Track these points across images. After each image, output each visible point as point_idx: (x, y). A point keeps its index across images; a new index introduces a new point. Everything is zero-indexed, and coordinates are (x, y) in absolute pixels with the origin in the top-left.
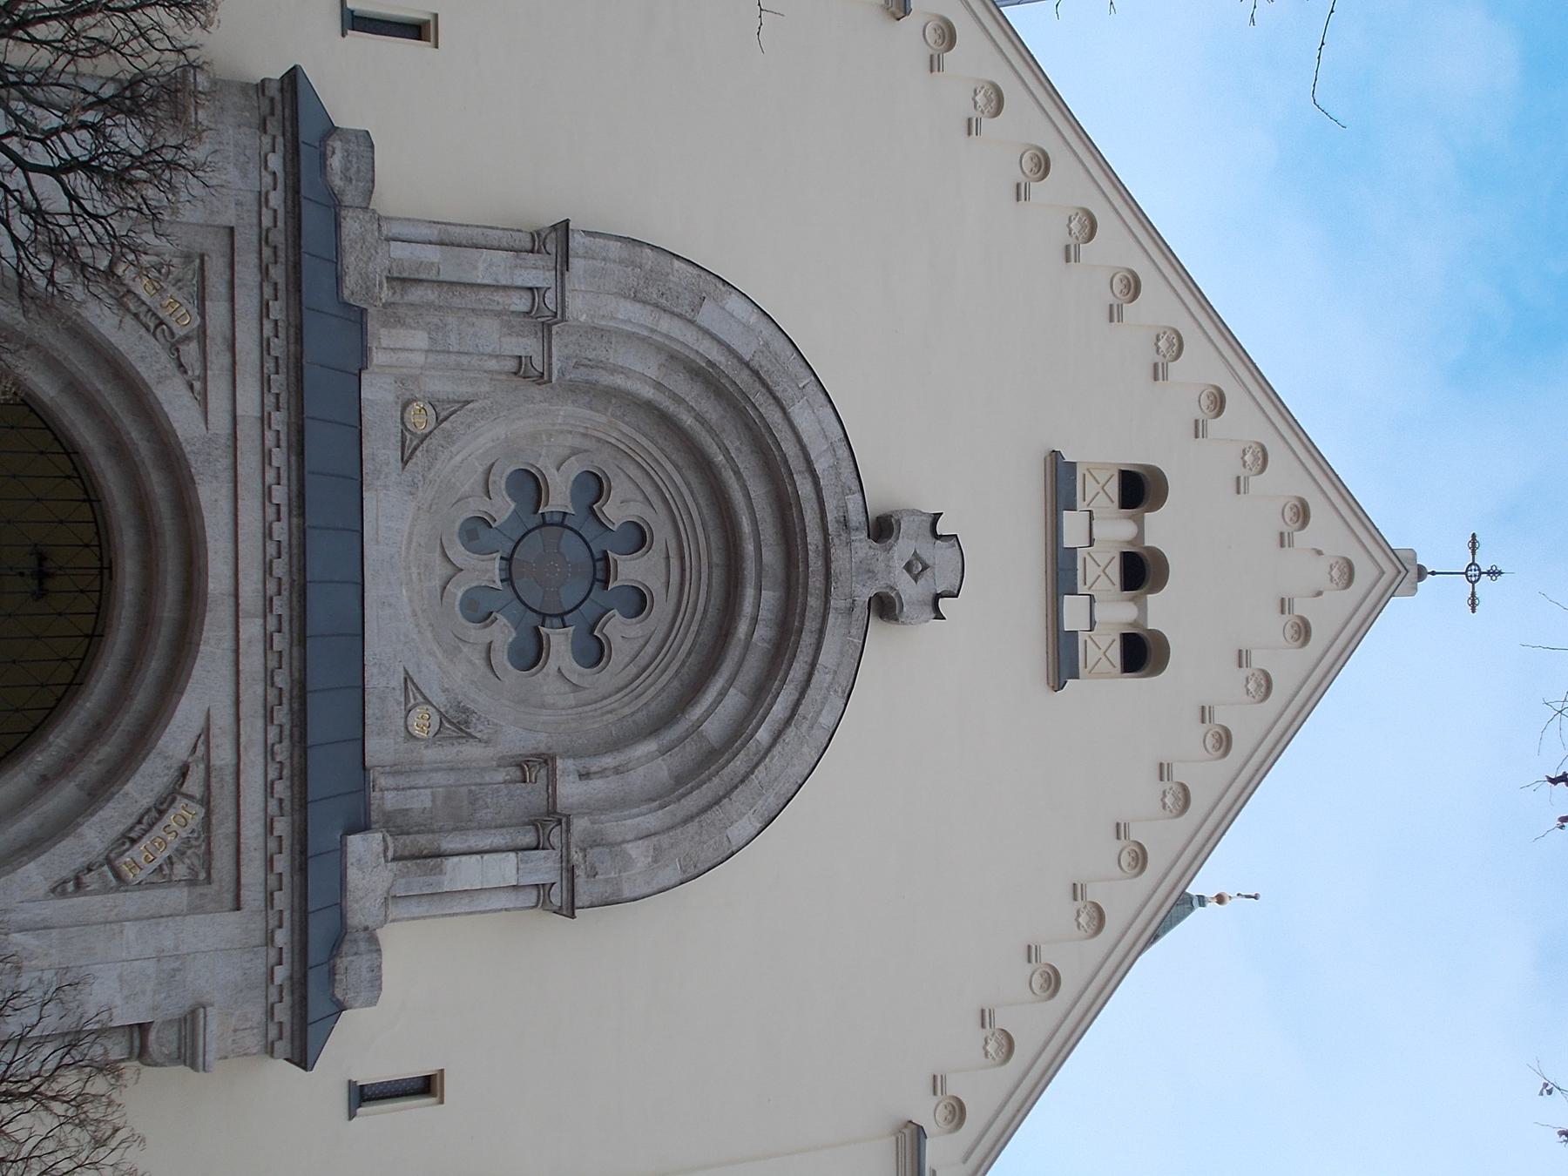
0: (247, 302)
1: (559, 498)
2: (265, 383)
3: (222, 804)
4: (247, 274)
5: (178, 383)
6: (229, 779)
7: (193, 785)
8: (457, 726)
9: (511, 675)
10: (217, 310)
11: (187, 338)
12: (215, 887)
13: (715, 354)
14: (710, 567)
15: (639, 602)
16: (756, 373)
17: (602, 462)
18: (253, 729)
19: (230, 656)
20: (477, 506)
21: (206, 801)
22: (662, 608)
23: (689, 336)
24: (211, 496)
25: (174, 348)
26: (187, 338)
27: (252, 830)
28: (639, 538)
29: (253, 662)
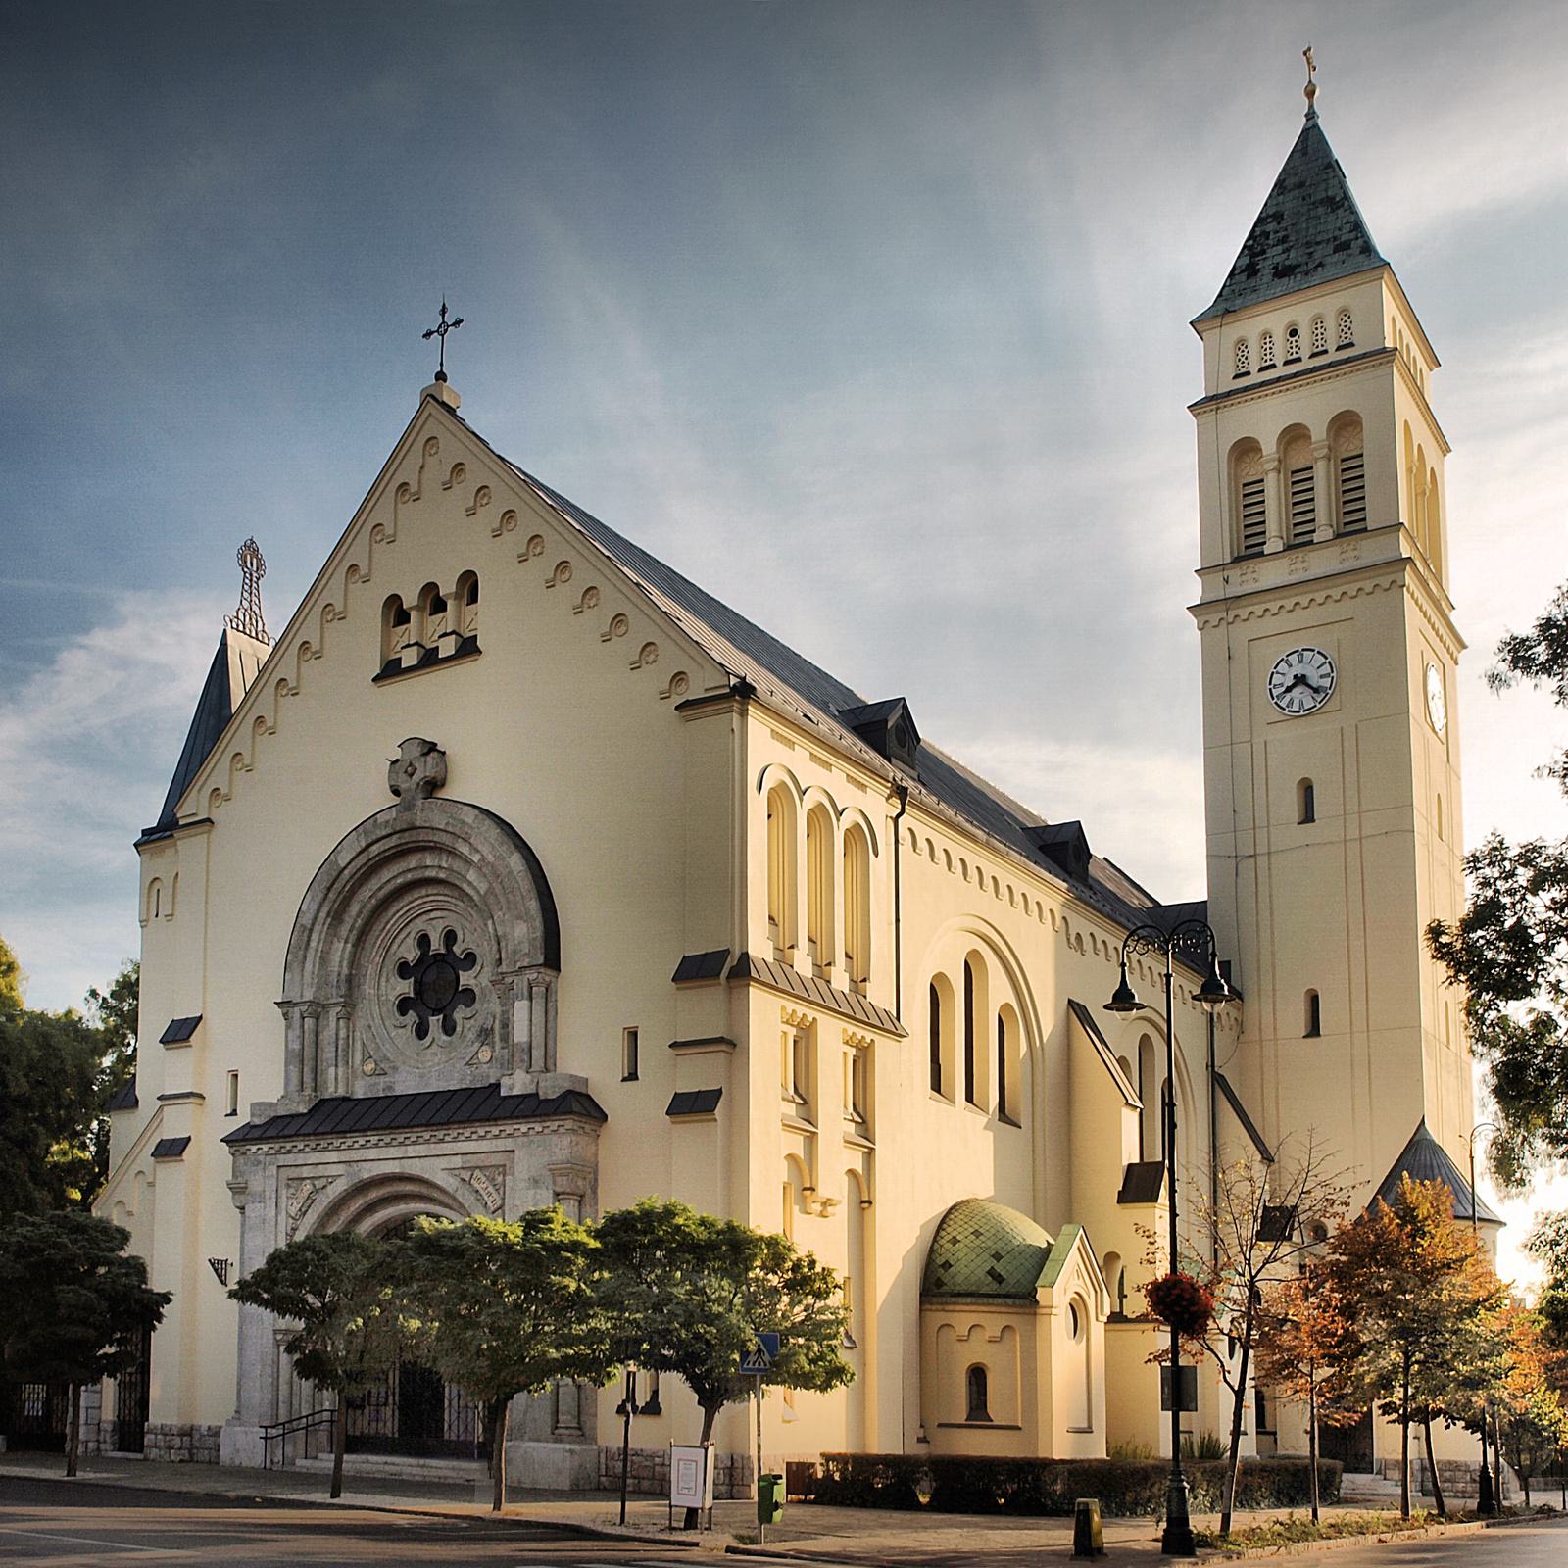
0: (300, 1159)
1: (406, 987)
2: (325, 1149)
3: (473, 1161)
4: (290, 1159)
5: (330, 1187)
6: (465, 1158)
7: (466, 1175)
8: (487, 1035)
9: (477, 1005)
10: (306, 1172)
11: (314, 1186)
12: (507, 1163)
13: (323, 915)
14: (428, 895)
15: (450, 937)
16: (329, 889)
17: (391, 966)
18: (446, 1148)
19: (422, 1160)
20: (409, 1033)
21: (473, 1169)
22: (452, 921)
23: (317, 928)
24: (367, 1172)
25: (317, 1191)
26: (314, 1186)
27: (485, 1145)
28: (424, 940)
29: (422, 1150)
